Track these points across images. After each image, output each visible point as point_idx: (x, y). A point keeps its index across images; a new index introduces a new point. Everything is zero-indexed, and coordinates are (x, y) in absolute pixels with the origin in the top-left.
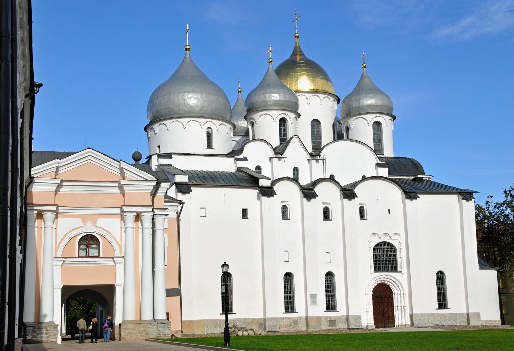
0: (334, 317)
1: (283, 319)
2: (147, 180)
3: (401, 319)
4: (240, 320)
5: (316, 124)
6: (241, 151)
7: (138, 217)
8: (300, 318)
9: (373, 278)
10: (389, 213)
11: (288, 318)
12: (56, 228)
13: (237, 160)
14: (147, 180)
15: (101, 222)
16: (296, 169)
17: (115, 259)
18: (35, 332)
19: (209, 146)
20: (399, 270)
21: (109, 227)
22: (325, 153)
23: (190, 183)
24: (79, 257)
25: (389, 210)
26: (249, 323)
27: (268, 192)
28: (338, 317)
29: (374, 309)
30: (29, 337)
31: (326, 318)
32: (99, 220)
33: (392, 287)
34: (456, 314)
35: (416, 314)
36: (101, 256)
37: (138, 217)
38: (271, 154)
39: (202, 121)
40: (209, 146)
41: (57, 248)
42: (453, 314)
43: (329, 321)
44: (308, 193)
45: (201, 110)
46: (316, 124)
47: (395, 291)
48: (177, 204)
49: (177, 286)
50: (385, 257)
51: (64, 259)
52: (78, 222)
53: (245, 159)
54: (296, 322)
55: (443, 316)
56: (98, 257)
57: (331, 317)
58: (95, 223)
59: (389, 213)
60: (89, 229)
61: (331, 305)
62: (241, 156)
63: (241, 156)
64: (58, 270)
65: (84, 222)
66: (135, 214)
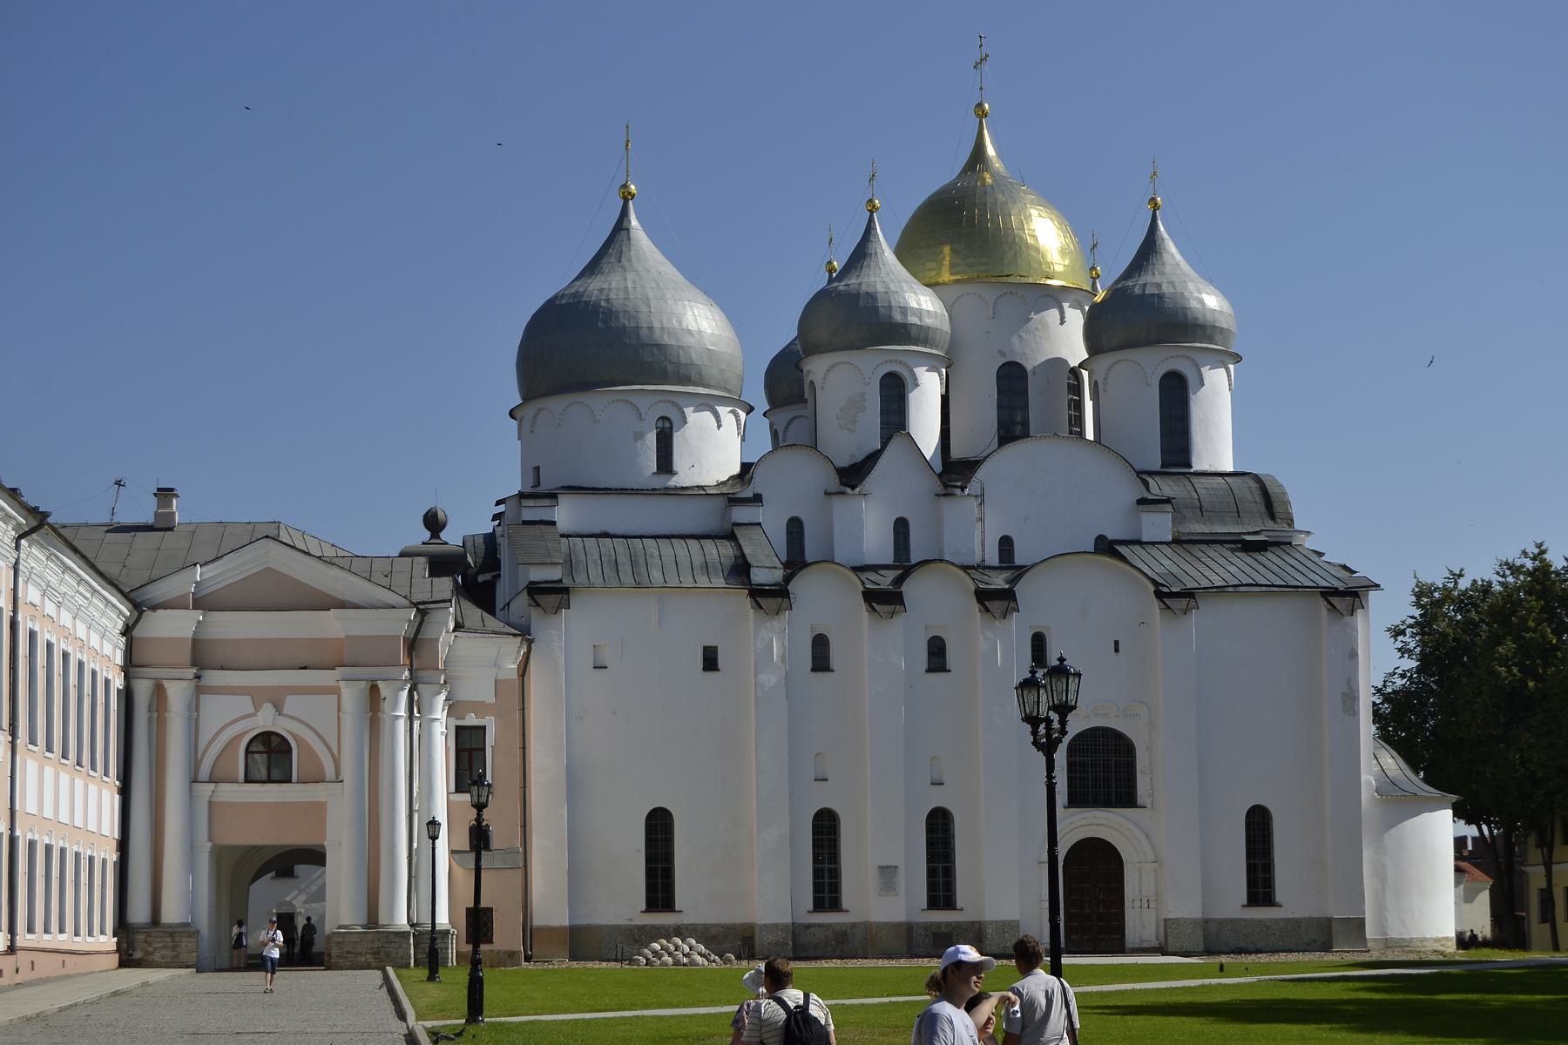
0: (948, 924)
1: (809, 926)
8: (854, 925)
10: (1117, 650)
11: (820, 925)
16: (901, 526)
18: (150, 944)
20: (1139, 801)
23: (567, 582)
24: (247, 781)
25: (1116, 643)
26: (715, 937)
30: (138, 955)
31: (928, 927)
34: (1297, 922)
35: (1176, 921)
38: (833, 481)
39: (643, 403)
40: (665, 463)
42: (1288, 920)
43: (935, 935)
51: (211, 786)
52: (245, 704)
53: (757, 499)
55: (1265, 925)
56: (289, 781)
59: (1117, 650)
60: (266, 720)
61: (827, 895)
66: (363, 685)
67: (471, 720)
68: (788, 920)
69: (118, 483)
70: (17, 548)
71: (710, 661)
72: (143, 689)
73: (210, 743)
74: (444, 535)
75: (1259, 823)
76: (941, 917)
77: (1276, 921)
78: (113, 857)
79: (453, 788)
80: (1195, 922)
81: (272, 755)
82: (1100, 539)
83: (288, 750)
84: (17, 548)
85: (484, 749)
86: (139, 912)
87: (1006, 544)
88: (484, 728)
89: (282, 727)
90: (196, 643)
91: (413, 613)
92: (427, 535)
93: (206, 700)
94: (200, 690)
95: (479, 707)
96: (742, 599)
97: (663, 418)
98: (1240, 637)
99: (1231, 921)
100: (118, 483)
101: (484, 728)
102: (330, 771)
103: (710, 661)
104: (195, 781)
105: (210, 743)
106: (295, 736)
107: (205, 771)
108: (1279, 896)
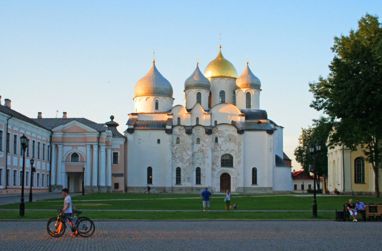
0: (199, 187)
1: (175, 187)
2: (95, 132)
3: (233, 189)
4: (155, 187)
5: (222, 94)
6: (170, 111)
7: (92, 146)
8: (183, 187)
9: (220, 170)
11: (177, 187)
12: (63, 151)
13: (168, 115)
14: (95, 132)
15: (79, 148)
16: (197, 119)
17: (84, 162)
19: (157, 108)
21: (81, 150)
22: (213, 110)
24: (72, 161)
27: (170, 132)
28: (201, 188)
29: (221, 184)
31: (195, 188)
32: (79, 147)
33: (230, 175)
34: (261, 189)
36: (79, 161)
37: (92, 146)
41: (63, 158)
42: (259, 188)
44: (189, 131)
45: (153, 92)
46: (222, 94)
47: (232, 177)
48: (123, 138)
49: (123, 172)
50: (227, 161)
51: (65, 162)
52: (70, 148)
53: (172, 114)
54: (181, 189)
55: (255, 189)
56: (78, 161)
57: (197, 187)
58: (77, 148)
60: (74, 151)
62: (171, 113)
63: (171, 113)
64: (64, 166)
65: (73, 148)
67: (116, 151)
68: (171, 186)
69: (57, 111)
70: (8, 121)
71: (159, 141)
72: (54, 146)
73: (65, 155)
74: (114, 120)
75: (254, 171)
76: (198, 186)
77: (257, 188)
78: (48, 173)
79: (112, 163)
80: (242, 188)
81: (75, 156)
82: (232, 121)
83: (78, 156)
84: (8, 121)
85: (117, 157)
86: (53, 183)
87: (216, 122)
88: (117, 153)
89: (77, 152)
90: (63, 138)
91: (98, 133)
92: (110, 120)
93: (65, 147)
94: (64, 146)
95: (117, 149)
96: (164, 132)
97: (157, 100)
98: (258, 139)
99: (249, 188)
100: (57, 111)
101: (117, 153)
102: (85, 161)
103: (159, 141)
104: (63, 161)
105: (65, 155)
106: (80, 154)
107: (64, 160)
108: (258, 183)
